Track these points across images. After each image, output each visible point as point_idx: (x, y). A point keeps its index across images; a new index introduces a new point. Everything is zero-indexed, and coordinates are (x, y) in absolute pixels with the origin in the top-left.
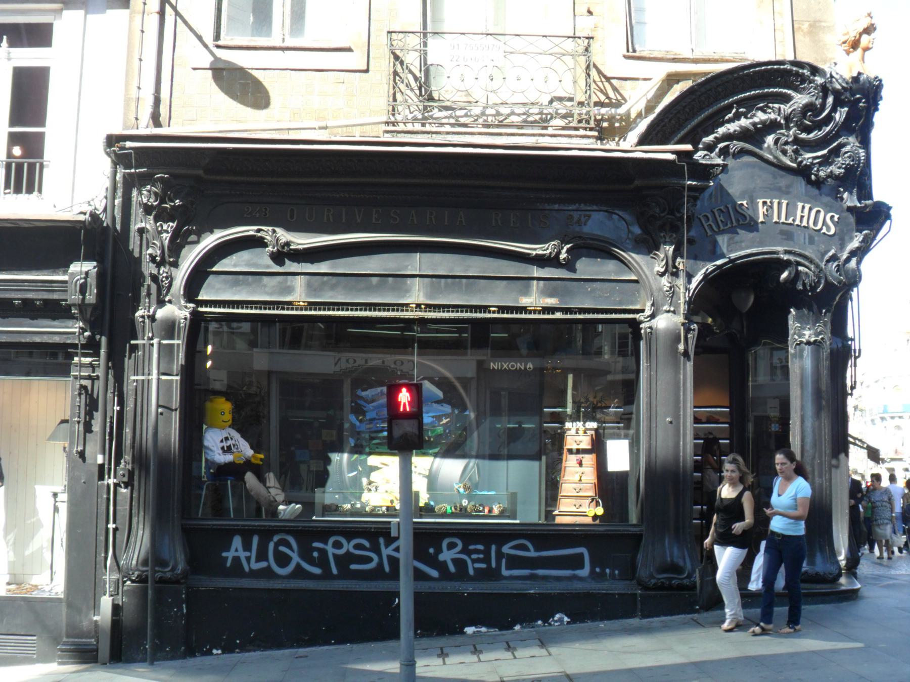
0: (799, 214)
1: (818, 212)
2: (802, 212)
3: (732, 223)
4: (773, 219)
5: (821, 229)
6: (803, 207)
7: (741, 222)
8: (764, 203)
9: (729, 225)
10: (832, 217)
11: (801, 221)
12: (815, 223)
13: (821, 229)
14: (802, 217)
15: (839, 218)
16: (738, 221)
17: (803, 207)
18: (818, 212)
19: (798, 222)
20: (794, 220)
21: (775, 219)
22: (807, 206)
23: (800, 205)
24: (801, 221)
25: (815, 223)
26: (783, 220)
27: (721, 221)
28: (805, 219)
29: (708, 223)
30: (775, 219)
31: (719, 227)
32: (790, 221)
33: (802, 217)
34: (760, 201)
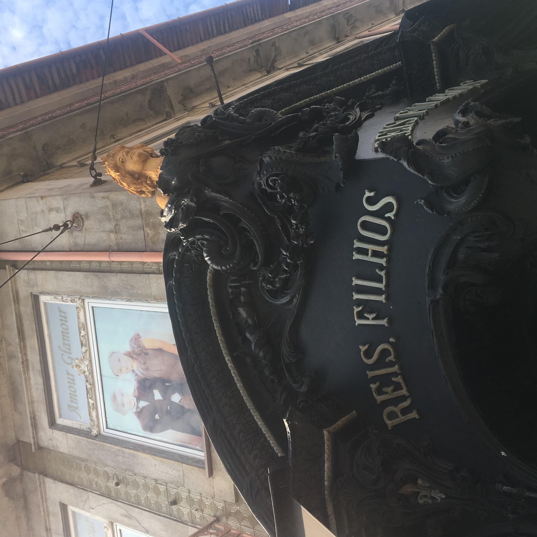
0: (369, 258)
1: (366, 226)
3: (395, 374)
5: (388, 219)
6: (362, 251)
7: (392, 358)
8: (361, 316)
9: (399, 379)
12: (382, 230)
13: (388, 219)
14: (375, 254)
15: (370, 191)
16: (391, 364)
17: (362, 251)
18: (366, 226)
19: (383, 261)
20: (381, 267)
21: (382, 298)
22: (357, 244)
23: (356, 256)
25: (382, 230)
27: (393, 391)
29: (399, 414)
32: (383, 273)
33: (375, 254)
34: (358, 322)
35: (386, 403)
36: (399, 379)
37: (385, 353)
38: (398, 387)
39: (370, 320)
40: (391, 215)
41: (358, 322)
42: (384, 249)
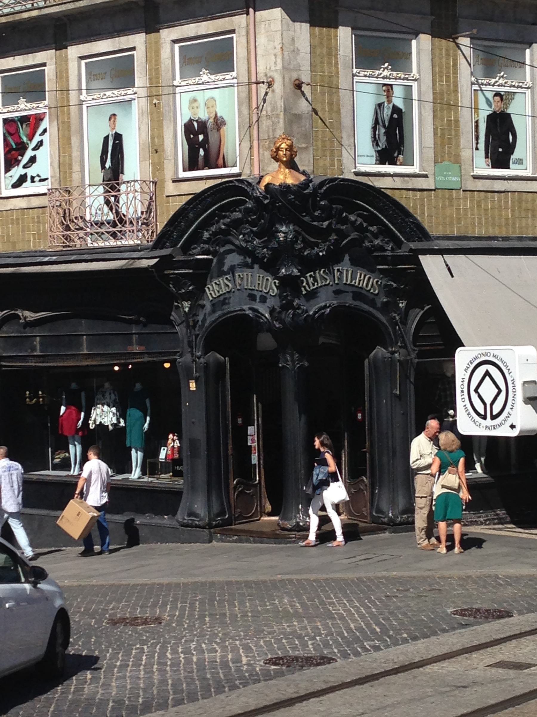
2: (360, 277)
4: (343, 281)
5: (370, 290)
8: (338, 270)
10: (377, 282)
11: (359, 284)
12: (367, 286)
14: (360, 281)
18: (369, 278)
19: (357, 284)
20: (355, 283)
24: (359, 284)
25: (367, 286)
26: (349, 282)
28: (361, 282)
30: (344, 282)
31: (215, 294)
32: (353, 283)
35: (306, 278)
36: (316, 286)
37: (326, 280)
38: (314, 285)
39: (337, 274)
40: (372, 291)
41: (336, 268)
42: (360, 285)
